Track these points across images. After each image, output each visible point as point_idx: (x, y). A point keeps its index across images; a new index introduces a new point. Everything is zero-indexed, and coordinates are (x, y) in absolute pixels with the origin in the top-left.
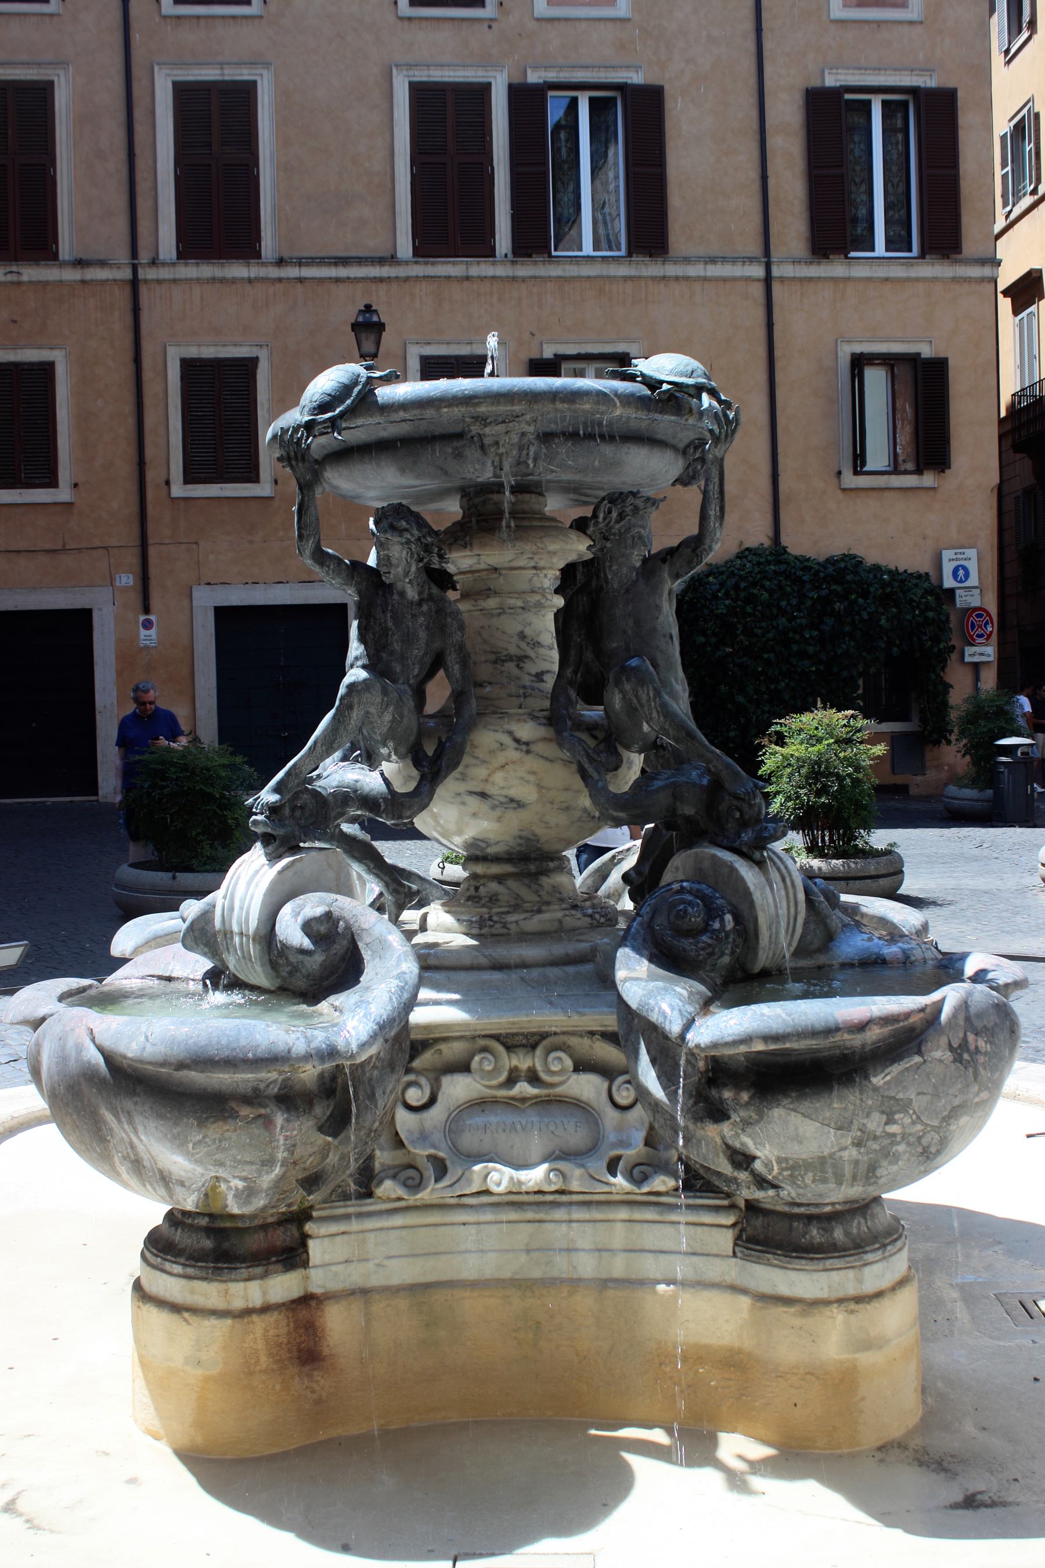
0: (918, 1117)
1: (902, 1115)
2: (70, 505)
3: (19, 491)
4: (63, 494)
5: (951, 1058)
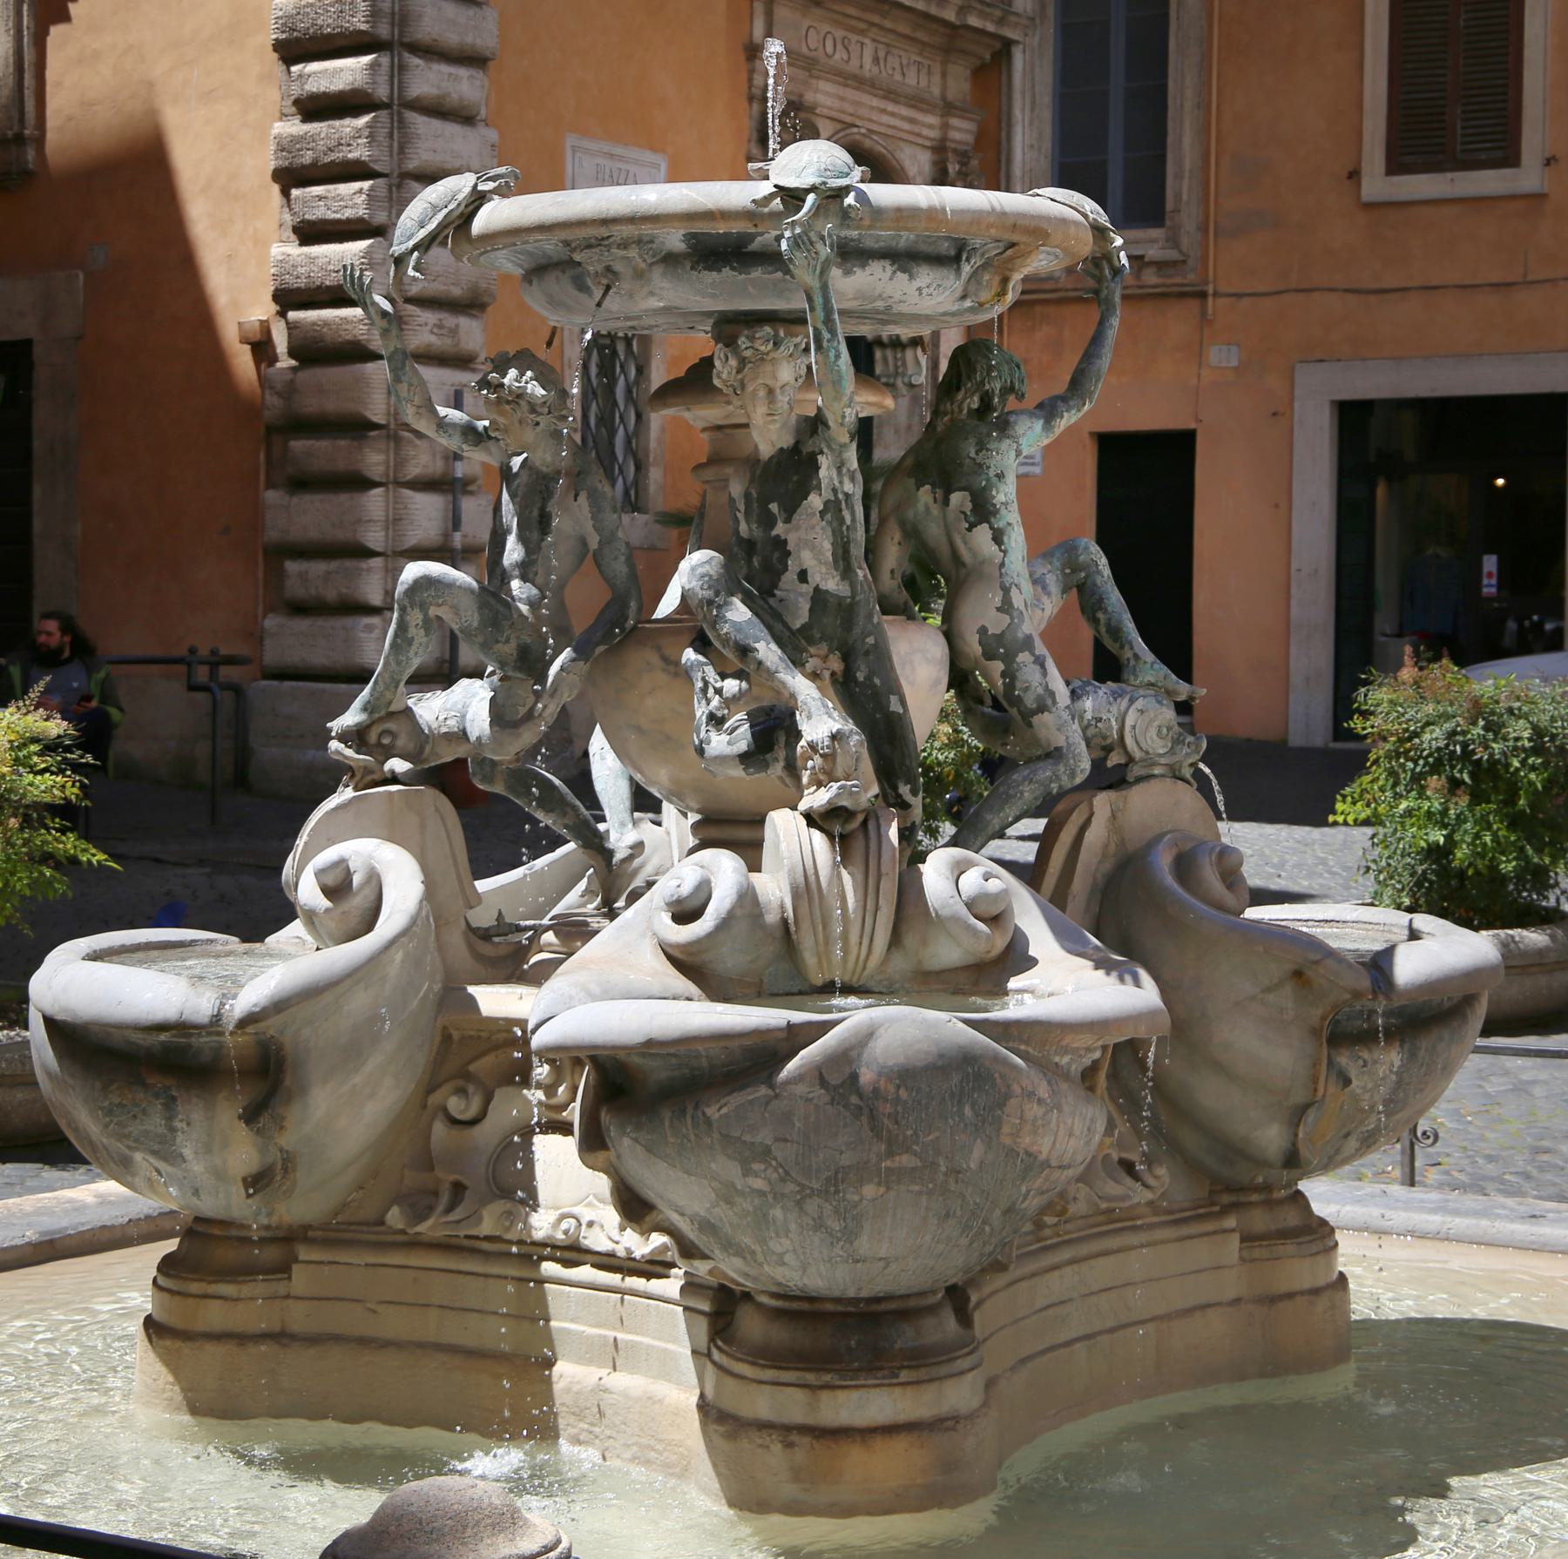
0: (787, 1173)
1: (763, 1167)
2: (1540, 197)
3: (1449, 175)
4: (1527, 177)
5: (827, 1099)
